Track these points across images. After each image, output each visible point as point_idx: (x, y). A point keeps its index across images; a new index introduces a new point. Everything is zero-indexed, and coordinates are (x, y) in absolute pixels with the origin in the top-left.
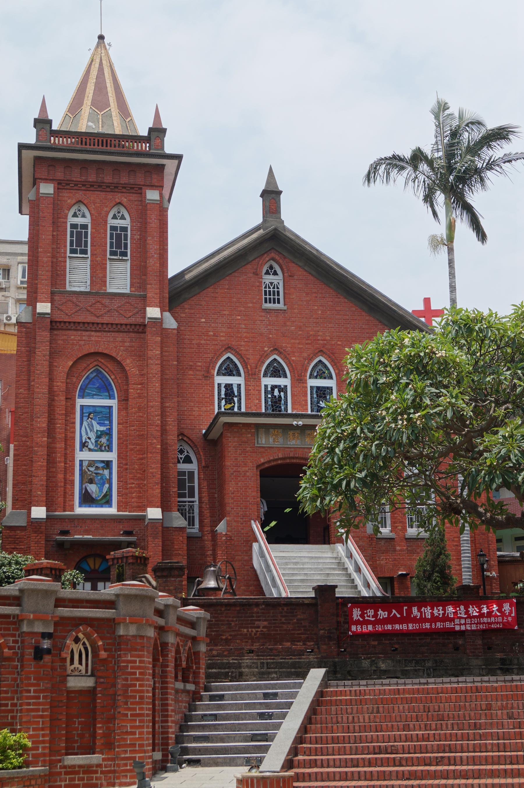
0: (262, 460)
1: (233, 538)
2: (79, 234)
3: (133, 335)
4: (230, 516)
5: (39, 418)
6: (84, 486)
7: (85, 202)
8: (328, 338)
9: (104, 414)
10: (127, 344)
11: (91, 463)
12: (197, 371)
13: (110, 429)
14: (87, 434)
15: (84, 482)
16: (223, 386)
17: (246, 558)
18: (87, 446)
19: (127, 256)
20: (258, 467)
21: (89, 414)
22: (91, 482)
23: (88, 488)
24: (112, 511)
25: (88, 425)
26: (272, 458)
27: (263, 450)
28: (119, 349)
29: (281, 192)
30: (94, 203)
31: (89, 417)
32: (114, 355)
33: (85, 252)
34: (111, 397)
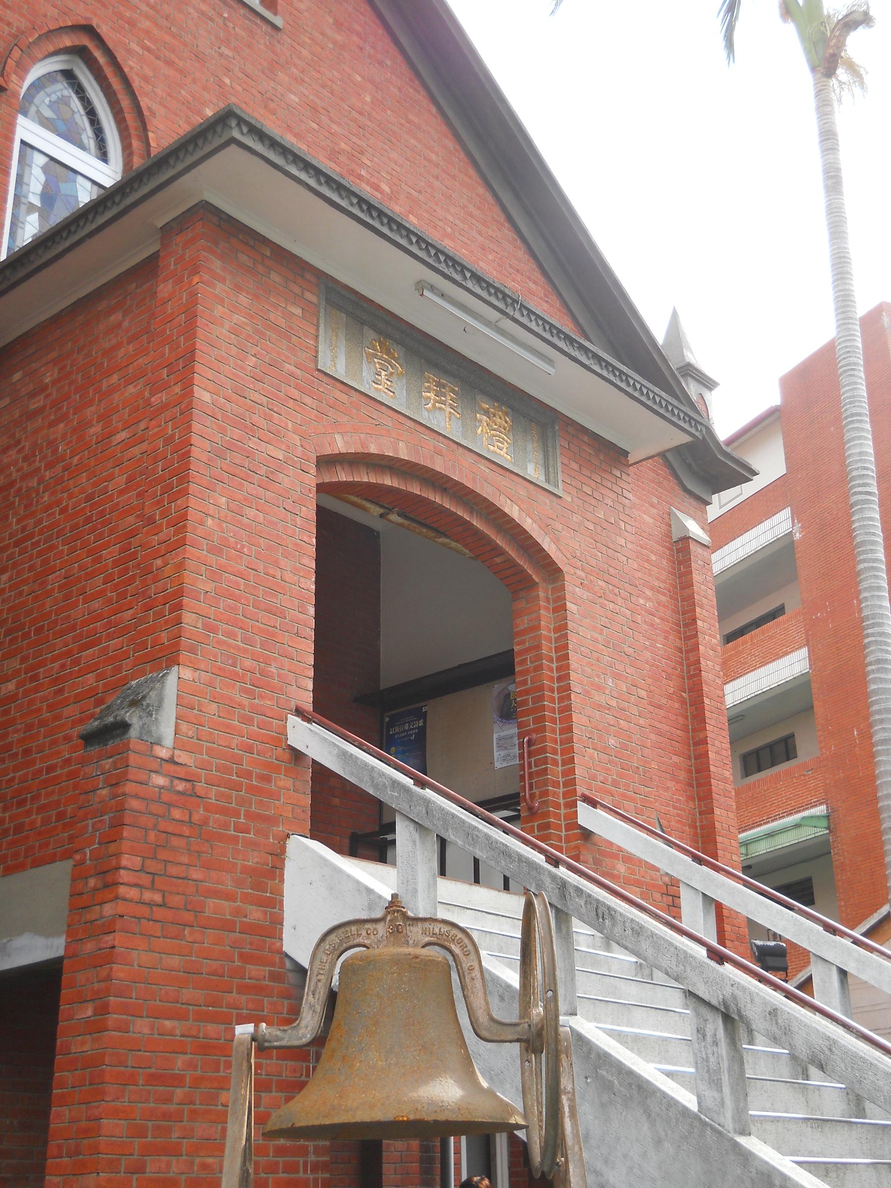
0: (341, 444)
1: (201, 787)
8: (386, 189)
17: (255, 914)
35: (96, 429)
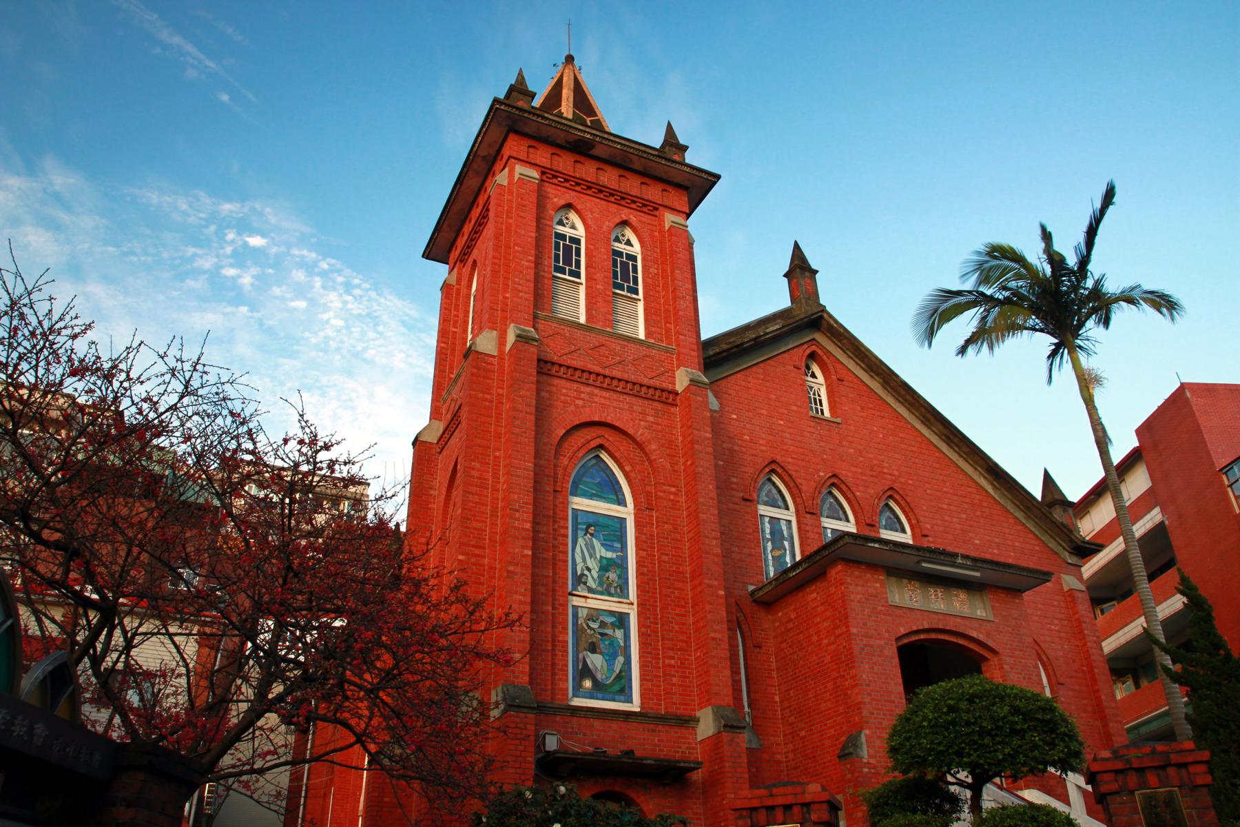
0: (902, 631)
2: (567, 250)
3: (659, 406)
4: (869, 728)
5: (517, 511)
6: (581, 656)
7: (579, 207)
8: (896, 473)
9: (612, 531)
10: (651, 419)
11: (594, 614)
12: (733, 489)
13: (624, 558)
14: (584, 560)
15: (581, 648)
16: (767, 519)
18: (585, 583)
19: (637, 293)
20: (898, 639)
21: (589, 526)
22: (593, 649)
23: (588, 661)
24: (635, 706)
25: (586, 545)
26: (915, 628)
27: (898, 612)
28: (639, 425)
29: (817, 272)
30: (592, 213)
31: (587, 532)
32: (631, 431)
33: (578, 275)
34: (621, 502)
35: (815, 638)
